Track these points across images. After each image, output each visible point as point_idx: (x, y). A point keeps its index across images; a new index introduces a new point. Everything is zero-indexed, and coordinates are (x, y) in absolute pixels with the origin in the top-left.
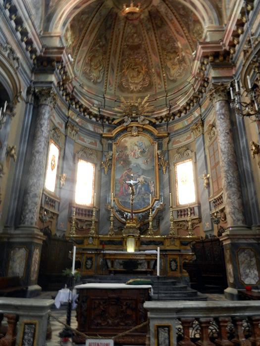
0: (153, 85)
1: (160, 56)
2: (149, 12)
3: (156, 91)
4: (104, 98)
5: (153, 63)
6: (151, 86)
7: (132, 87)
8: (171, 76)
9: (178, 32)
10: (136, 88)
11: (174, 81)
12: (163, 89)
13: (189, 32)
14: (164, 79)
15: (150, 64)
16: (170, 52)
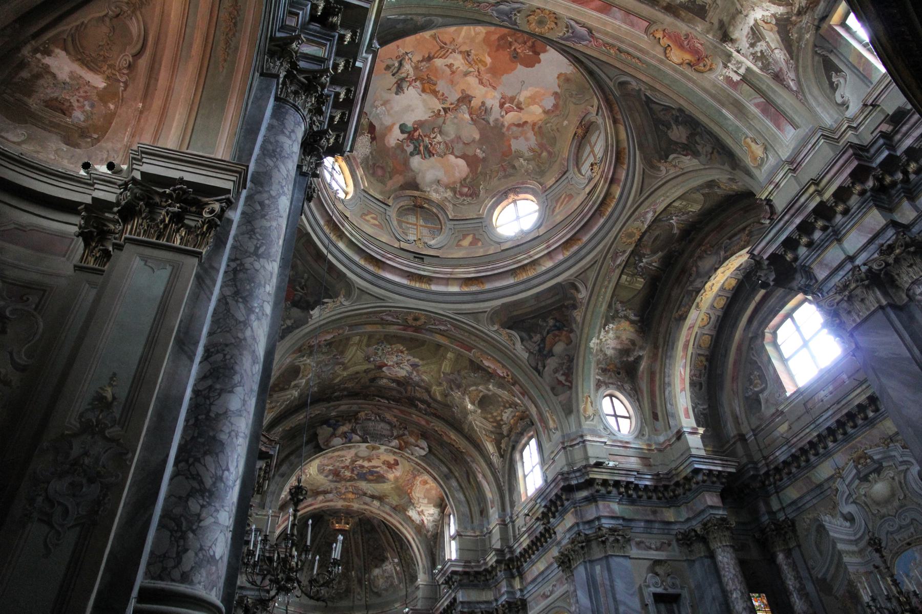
0: (350, 592)
1: (364, 559)
2: (360, 519)
3: (354, 601)
4: (287, 610)
5: (355, 566)
6: (348, 591)
7: (322, 592)
8: (375, 587)
9: (389, 544)
10: (328, 593)
11: (378, 594)
12: (363, 602)
13: (401, 548)
14: (366, 588)
15: (351, 565)
16: (376, 558)
